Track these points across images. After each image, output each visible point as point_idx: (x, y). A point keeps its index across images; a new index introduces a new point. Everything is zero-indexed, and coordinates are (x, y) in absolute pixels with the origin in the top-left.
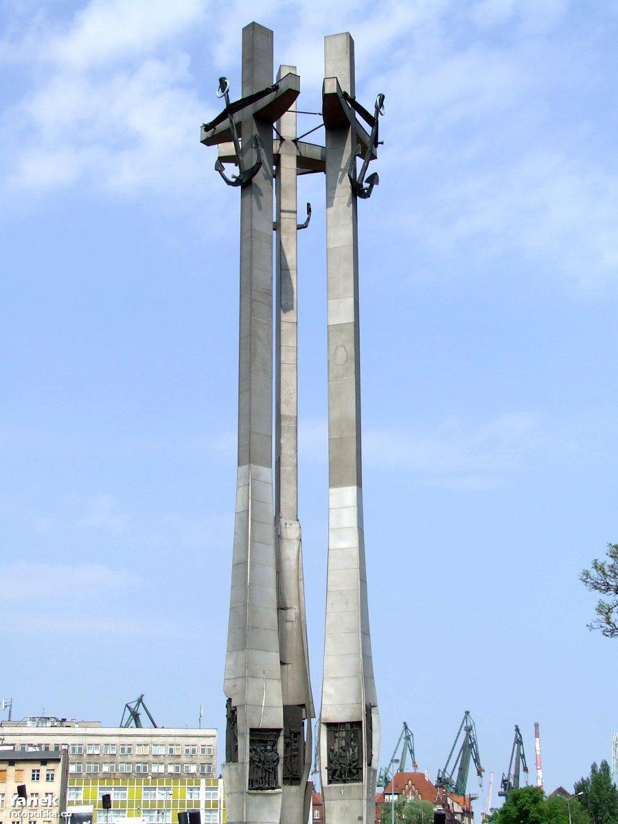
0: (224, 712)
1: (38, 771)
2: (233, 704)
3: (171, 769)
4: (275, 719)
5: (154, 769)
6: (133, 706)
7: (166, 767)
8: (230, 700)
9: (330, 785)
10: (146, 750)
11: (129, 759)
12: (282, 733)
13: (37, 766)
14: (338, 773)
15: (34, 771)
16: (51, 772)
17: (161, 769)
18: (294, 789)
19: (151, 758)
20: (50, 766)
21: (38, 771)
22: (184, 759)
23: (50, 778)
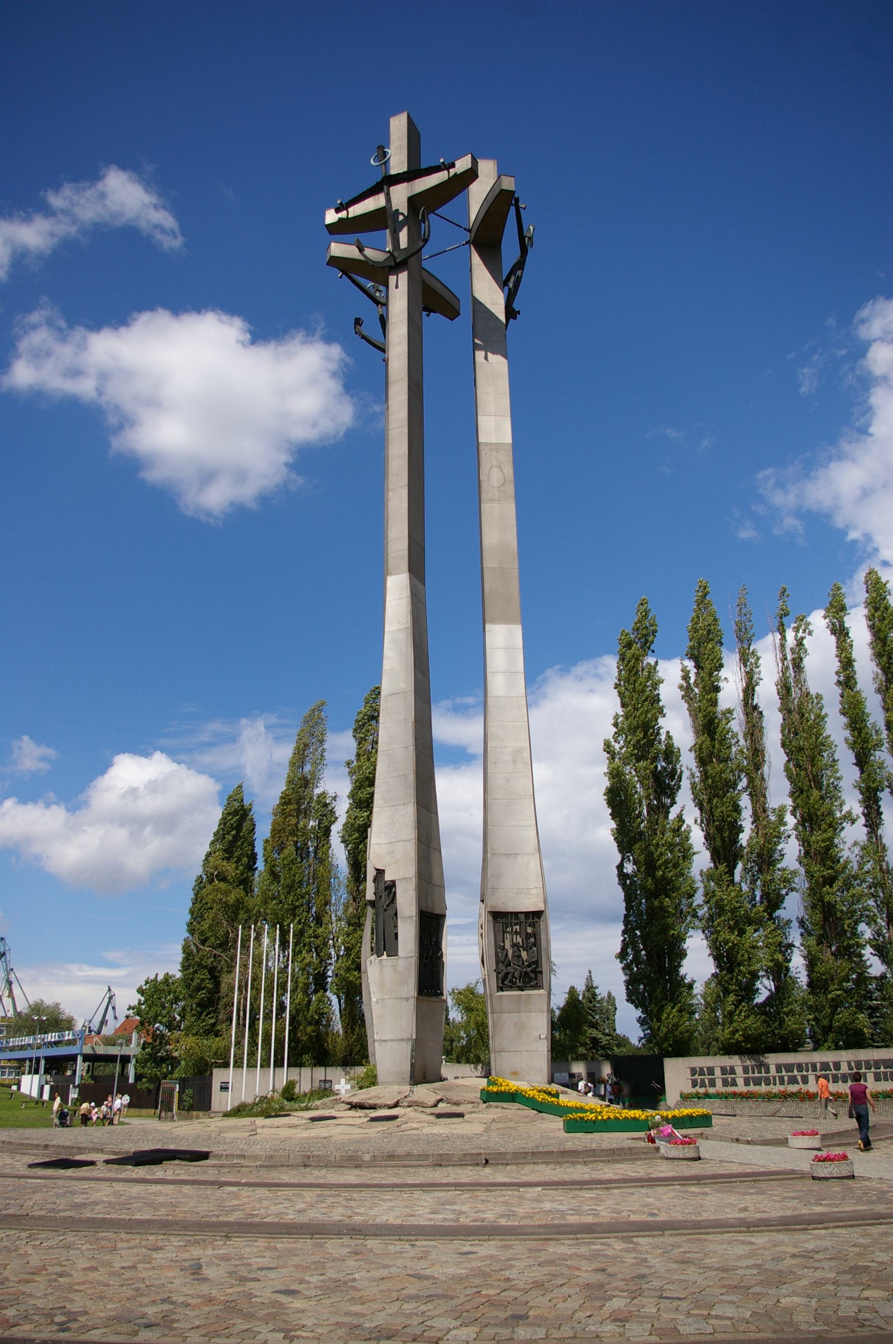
2: (388, 877)
9: (500, 993)
14: (510, 976)
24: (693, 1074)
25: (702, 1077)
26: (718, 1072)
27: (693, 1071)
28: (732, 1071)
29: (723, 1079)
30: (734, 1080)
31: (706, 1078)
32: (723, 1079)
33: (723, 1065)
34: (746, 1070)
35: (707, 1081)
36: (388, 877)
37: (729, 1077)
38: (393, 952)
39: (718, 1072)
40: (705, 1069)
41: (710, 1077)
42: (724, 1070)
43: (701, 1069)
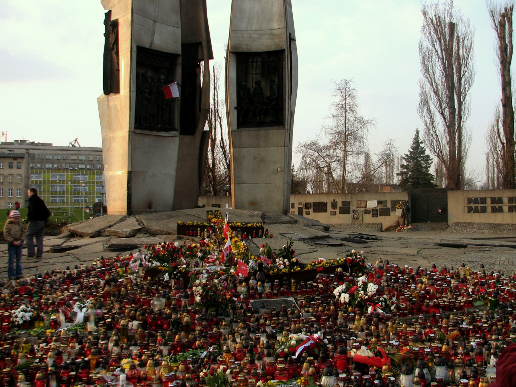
0: (102, 29)
1: (12, 163)
2: (113, 18)
3: (88, 167)
4: (167, 38)
5: (80, 166)
6: (73, 143)
7: (86, 166)
8: (108, 15)
10: (75, 157)
11: (67, 161)
12: (180, 61)
13: (11, 160)
15: (10, 163)
16: (19, 164)
17: (84, 166)
18: (187, 139)
19: (78, 161)
20: (19, 160)
21: (12, 163)
22: (94, 162)
23: (19, 168)
24: (469, 203)
25: (476, 205)
26: (489, 201)
27: (470, 201)
28: (500, 201)
29: (492, 207)
30: (501, 207)
31: (479, 206)
32: (492, 207)
33: (493, 196)
34: (511, 200)
35: (479, 208)
36: (113, 18)
37: (497, 205)
38: (117, 91)
39: (489, 201)
40: (479, 199)
41: (482, 205)
42: (493, 200)
43: (476, 199)
